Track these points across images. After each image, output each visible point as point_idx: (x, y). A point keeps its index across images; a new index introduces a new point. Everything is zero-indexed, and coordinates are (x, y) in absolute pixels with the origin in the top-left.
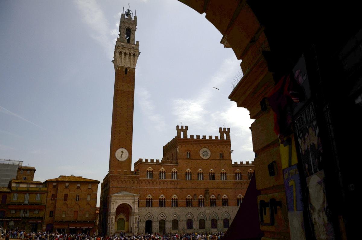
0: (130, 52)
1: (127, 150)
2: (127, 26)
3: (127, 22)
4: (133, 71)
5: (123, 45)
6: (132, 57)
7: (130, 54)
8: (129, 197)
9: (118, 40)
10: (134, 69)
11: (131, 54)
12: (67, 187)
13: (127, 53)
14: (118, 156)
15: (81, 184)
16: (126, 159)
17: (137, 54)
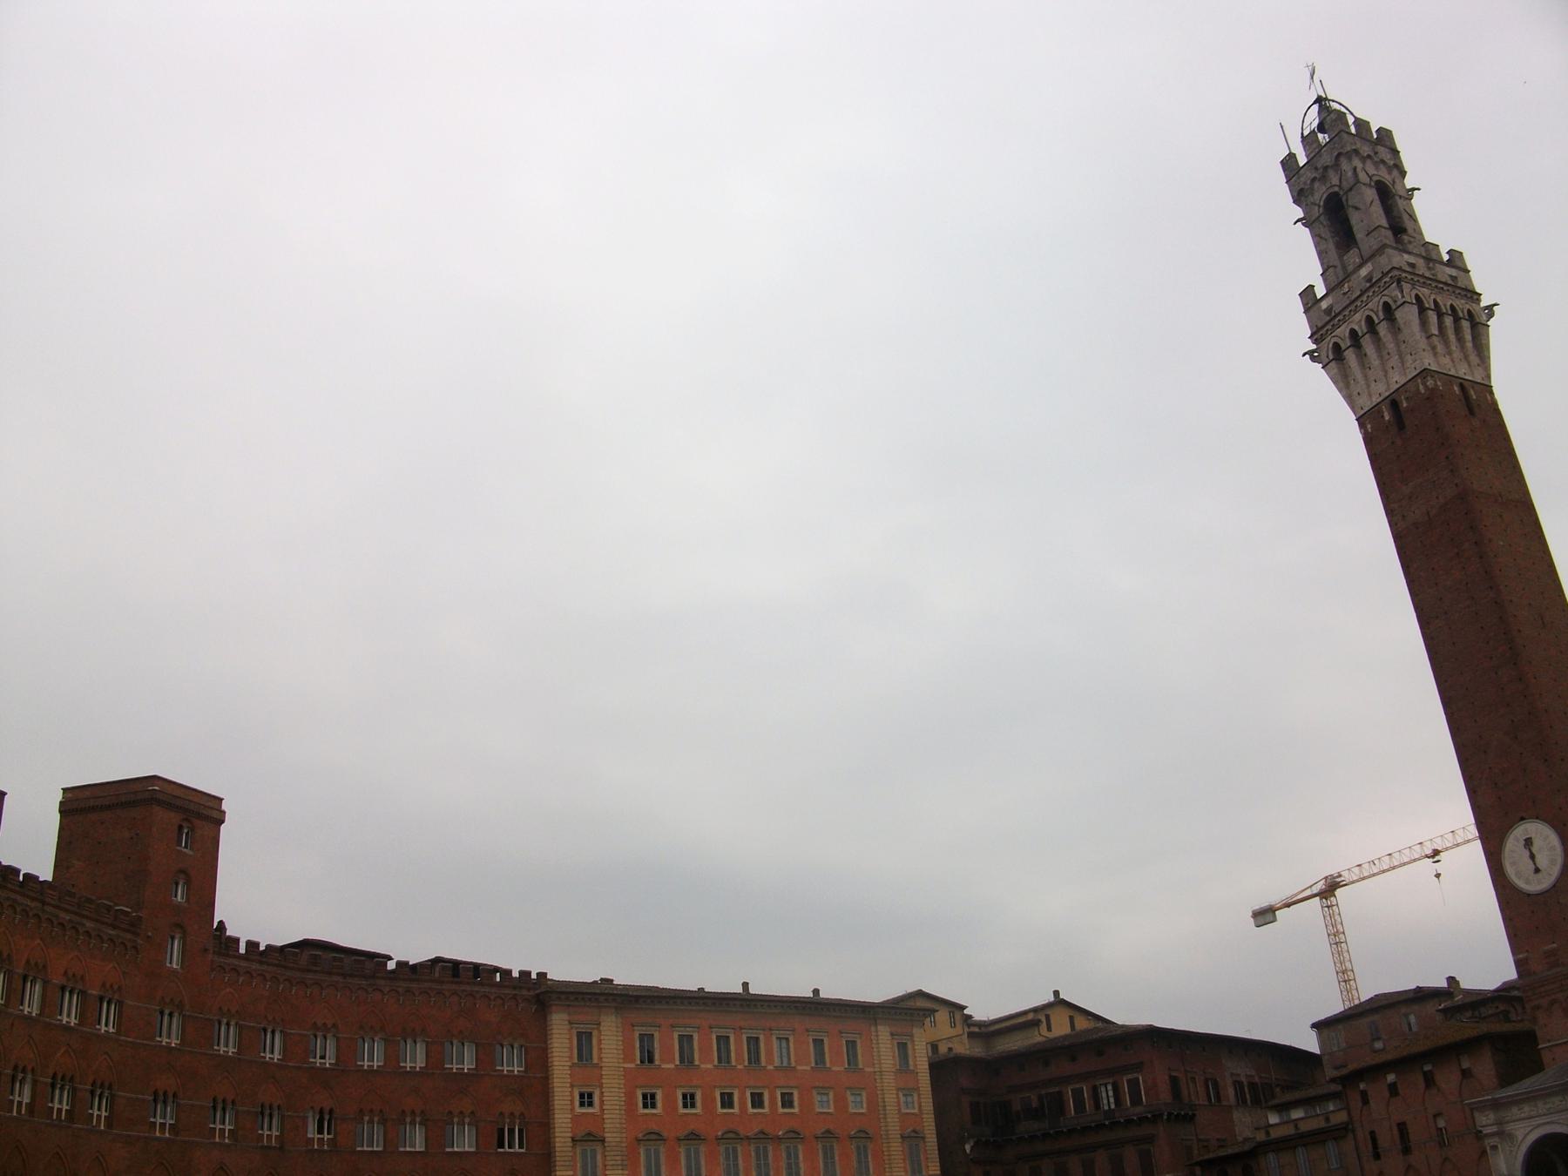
0: (1367, 313)
1: (1545, 820)
2: (1320, 194)
3: (1314, 180)
4: (1421, 387)
5: (1328, 311)
6: (1383, 329)
7: (1369, 320)
8: (1560, 1098)
9: (1307, 304)
10: (1425, 373)
11: (1375, 318)
12: (1393, 1089)
13: (1356, 328)
14: (1518, 874)
15: (1433, 1066)
16: (1556, 871)
17: (1393, 295)
